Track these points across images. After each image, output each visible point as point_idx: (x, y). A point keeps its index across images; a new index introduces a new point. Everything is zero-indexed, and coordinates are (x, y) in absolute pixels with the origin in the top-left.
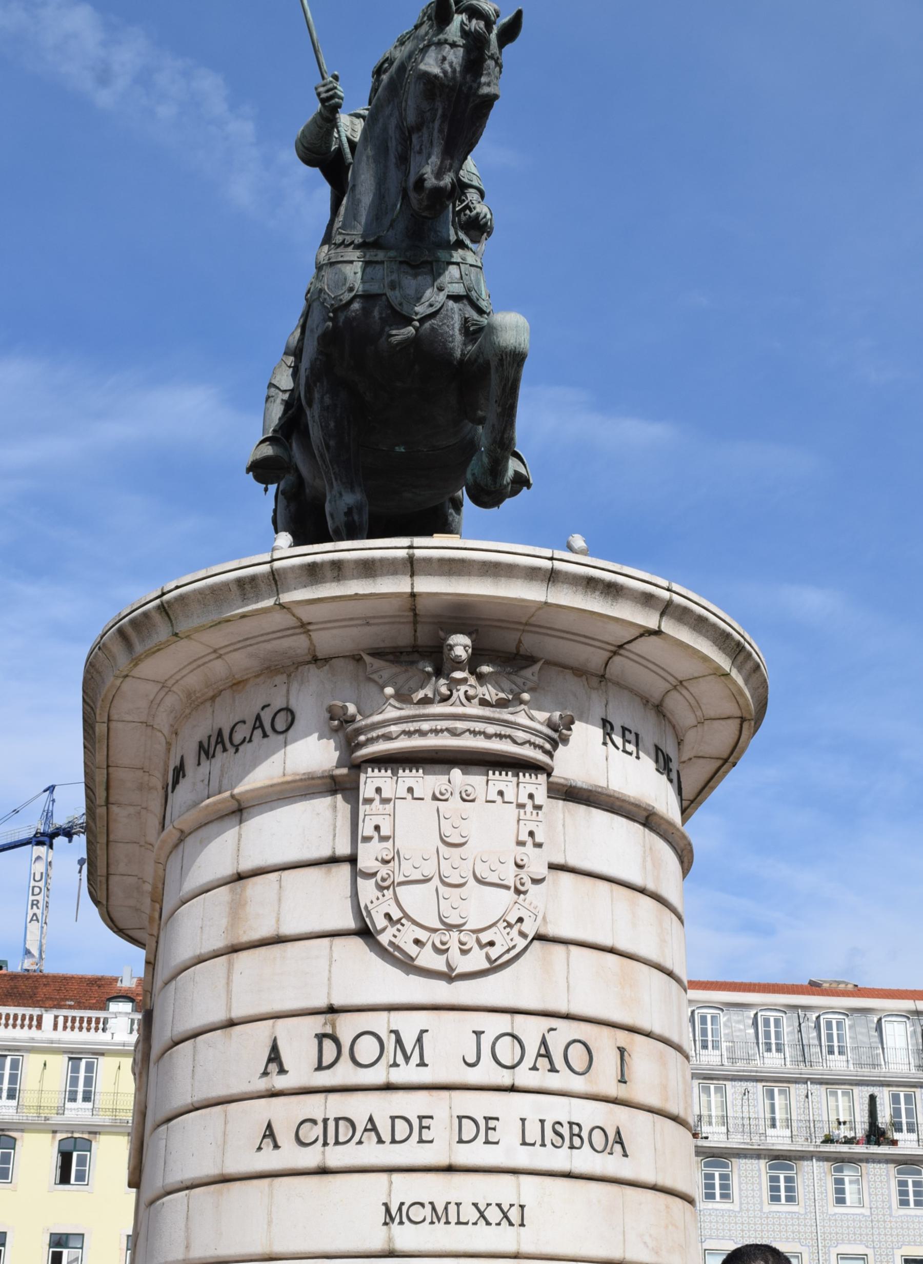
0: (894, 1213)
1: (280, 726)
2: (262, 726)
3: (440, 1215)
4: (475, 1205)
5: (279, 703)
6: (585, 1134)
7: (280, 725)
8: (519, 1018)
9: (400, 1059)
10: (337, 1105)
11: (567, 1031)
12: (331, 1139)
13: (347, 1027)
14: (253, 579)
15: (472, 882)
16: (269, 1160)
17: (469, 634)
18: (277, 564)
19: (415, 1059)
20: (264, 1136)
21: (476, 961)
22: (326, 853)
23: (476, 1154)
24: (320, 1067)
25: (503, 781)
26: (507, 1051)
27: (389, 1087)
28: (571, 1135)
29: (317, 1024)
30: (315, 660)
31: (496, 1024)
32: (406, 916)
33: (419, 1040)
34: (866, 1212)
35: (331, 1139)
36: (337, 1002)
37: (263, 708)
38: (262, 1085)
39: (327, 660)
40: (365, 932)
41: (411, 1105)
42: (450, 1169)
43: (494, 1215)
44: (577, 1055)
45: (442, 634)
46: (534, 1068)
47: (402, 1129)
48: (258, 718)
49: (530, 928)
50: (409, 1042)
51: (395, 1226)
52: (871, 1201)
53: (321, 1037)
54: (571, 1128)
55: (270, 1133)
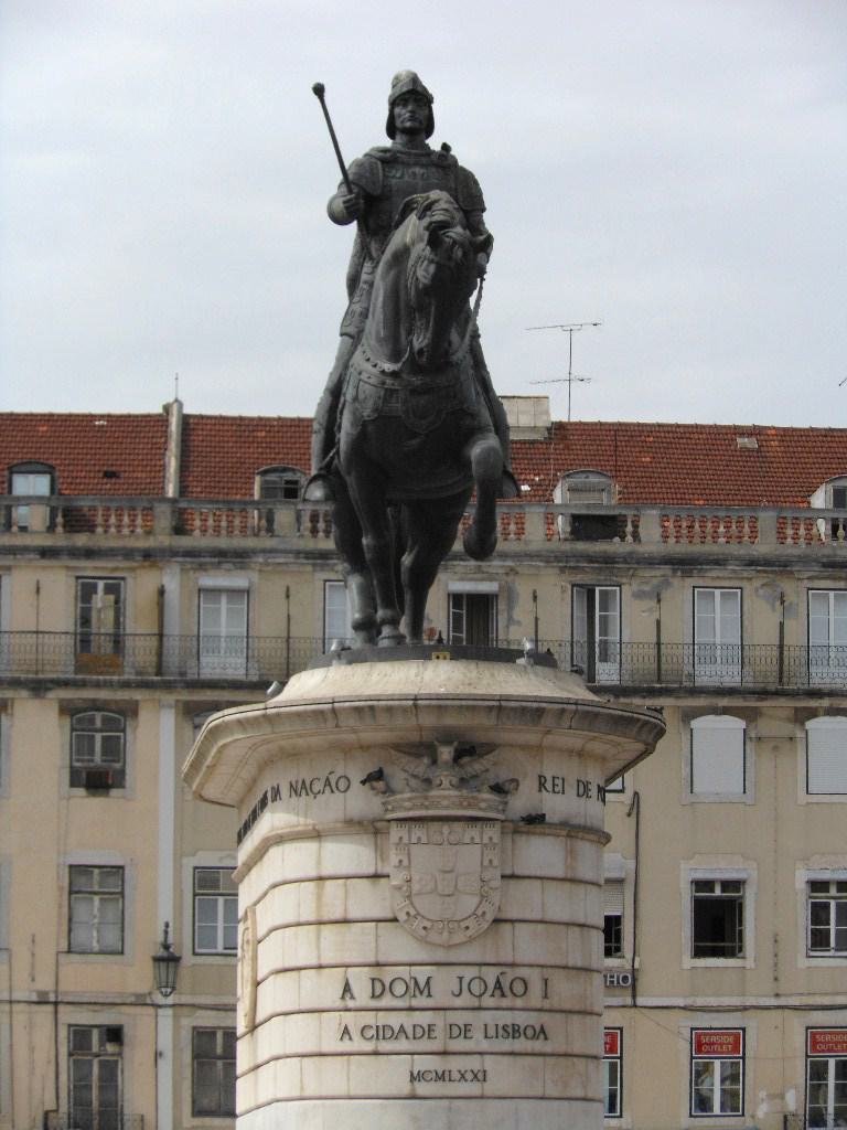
1: (342, 787)
2: (330, 785)
3: (441, 1077)
4: (460, 1071)
5: (340, 771)
6: (521, 1030)
7: (342, 787)
8: (484, 968)
9: (417, 993)
10: (383, 1019)
11: (511, 973)
12: (381, 1037)
13: (388, 975)
14: (322, 712)
16: (346, 1046)
18: (336, 705)
21: (459, 938)
22: (371, 871)
23: (459, 1044)
25: (473, 832)
27: (411, 1009)
28: (514, 1031)
29: (374, 973)
31: (469, 973)
32: (418, 914)
35: (381, 1037)
36: (382, 959)
37: (330, 773)
38: (339, 1004)
40: (395, 920)
41: (423, 1019)
42: (445, 1053)
44: (519, 987)
45: (436, 743)
46: (493, 995)
48: (328, 779)
49: (490, 917)
50: (422, 986)
51: (416, 1083)
54: (513, 1028)
55: (346, 1031)
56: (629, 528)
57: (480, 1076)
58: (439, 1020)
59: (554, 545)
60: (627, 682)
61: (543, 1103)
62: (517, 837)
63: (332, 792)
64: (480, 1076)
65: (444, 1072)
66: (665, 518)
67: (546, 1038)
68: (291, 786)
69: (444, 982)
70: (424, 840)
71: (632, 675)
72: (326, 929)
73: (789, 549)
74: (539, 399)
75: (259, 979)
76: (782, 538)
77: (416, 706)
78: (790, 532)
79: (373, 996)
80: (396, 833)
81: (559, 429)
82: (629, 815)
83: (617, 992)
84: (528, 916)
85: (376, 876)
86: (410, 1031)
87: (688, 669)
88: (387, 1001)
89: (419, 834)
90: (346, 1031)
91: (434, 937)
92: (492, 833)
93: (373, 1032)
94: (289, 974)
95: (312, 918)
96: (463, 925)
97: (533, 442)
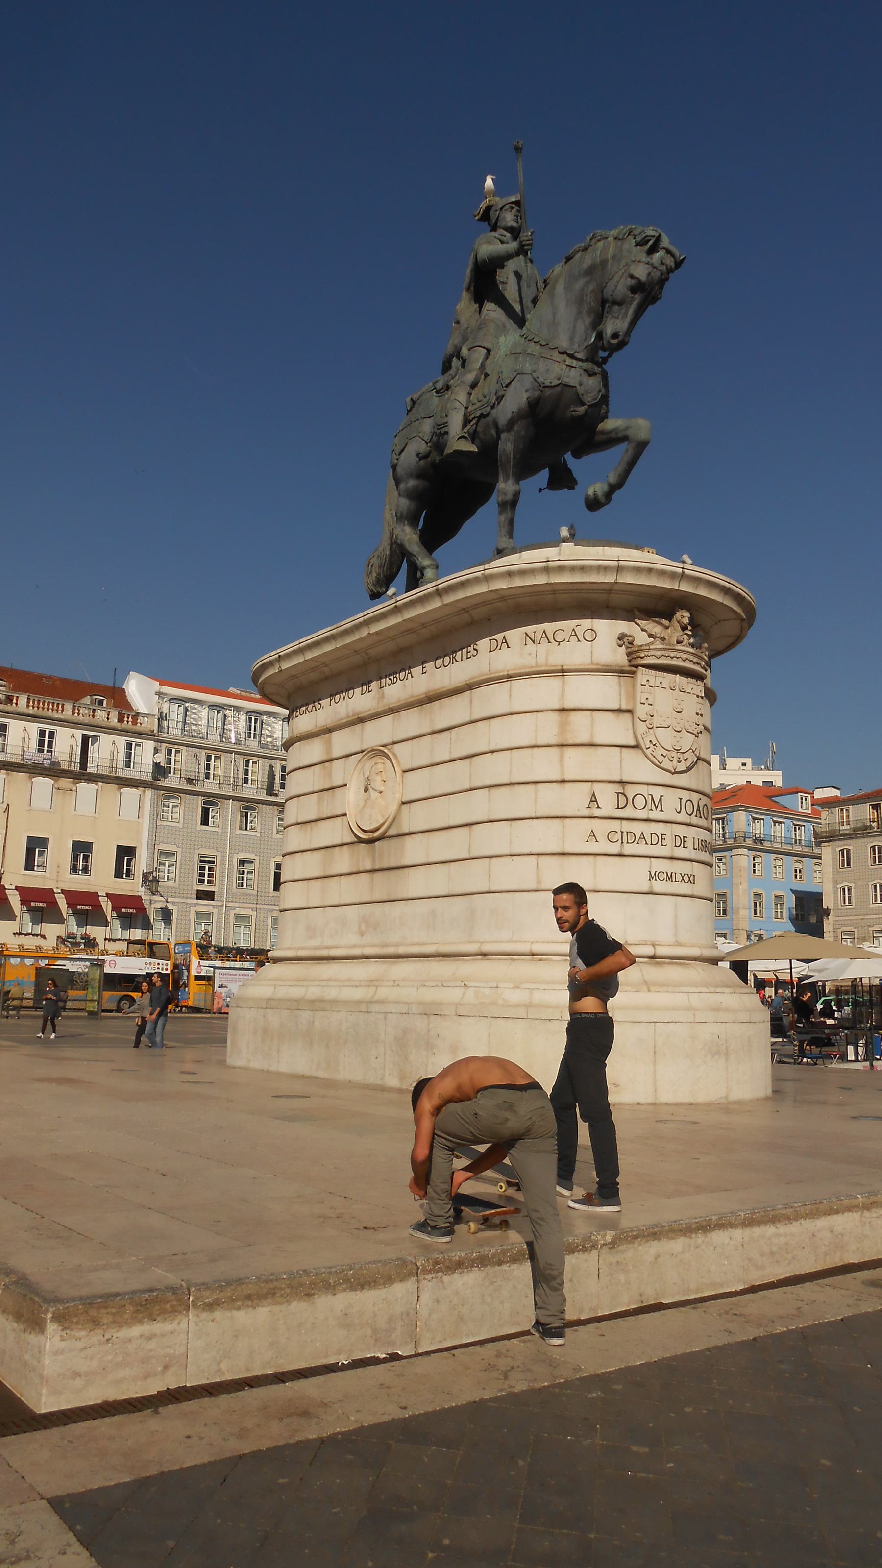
10: (626, 826)
12: (625, 841)
13: (631, 791)
15: (684, 731)
17: (689, 610)
21: (682, 767)
22: (616, 707)
24: (618, 808)
30: (607, 607)
31: (686, 795)
33: (660, 800)
38: (587, 812)
39: (615, 608)
40: (637, 746)
41: (659, 829)
43: (686, 879)
51: (653, 881)
53: (618, 793)
56: (15, 701)
64: (691, 880)
66: (29, 699)
69: (671, 799)
76: (73, 714)
77: (683, 572)
78: (77, 711)
80: (643, 675)
85: (619, 711)
89: (661, 680)
91: (667, 764)
93: (619, 836)
96: (686, 756)
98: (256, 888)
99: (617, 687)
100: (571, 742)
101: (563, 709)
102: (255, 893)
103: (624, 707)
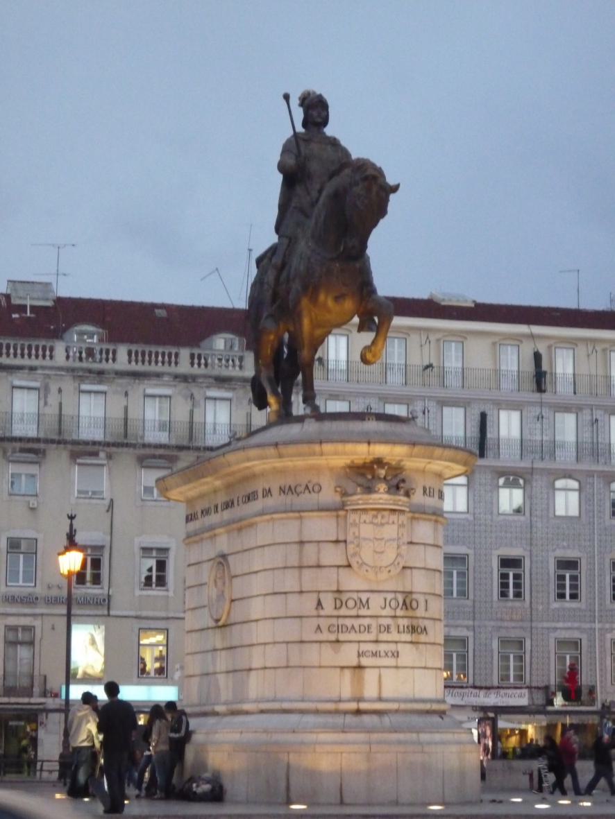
0: (494, 517)
2: (308, 488)
5: (315, 480)
7: (316, 488)
9: (361, 607)
10: (341, 621)
13: (344, 597)
19: (366, 607)
20: (317, 629)
22: (334, 538)
23: (384, 637)
25: (394, 518)
26: (393, 604)
27: (358, 616)
31: (389, 596)
33: (367, 601)
34: (470, 517)
38: (315, 613)
40: (349, 566)
41: (366, 622)
42: (377, 641)
47: (362, 628)
49: (401, 566)
50: (364, 601)
51: (361, 659)
52: (474, 508)
55: (319, 627)
57: (395, 654)
58: (373, 622)
59: (70, 363)
60: (109, 439)
61: (426, 671)
62: (415, 522)
63: (310, 492)
64: (396, 655)
65: (376, 652)
67: (427, 633)
68: (280, 488)
70: (368, 521)
71: (112, 435)
72: (306, 572)
73: (196, 370)
74: (48, 285)
75: (233, 598)
76: (192, 364)
79: (336, 608)
81: (60, 301)
82: (108, 511)
83: (100, 607)
84: (418, 565)
85: (337, 542)
86: (357, 629)
87: (140, 433)
88: (343, 611)
90: (319, 627)
92: (403, 518)
93: (336, 628)
94: (277, 596)
95: (296, 564)
97: (47, 308)
98: (471, 597)
99: (335, 525)
100: (305, 564)
101: (301, 543)
102: (469, 603)
103: (341, 538)
